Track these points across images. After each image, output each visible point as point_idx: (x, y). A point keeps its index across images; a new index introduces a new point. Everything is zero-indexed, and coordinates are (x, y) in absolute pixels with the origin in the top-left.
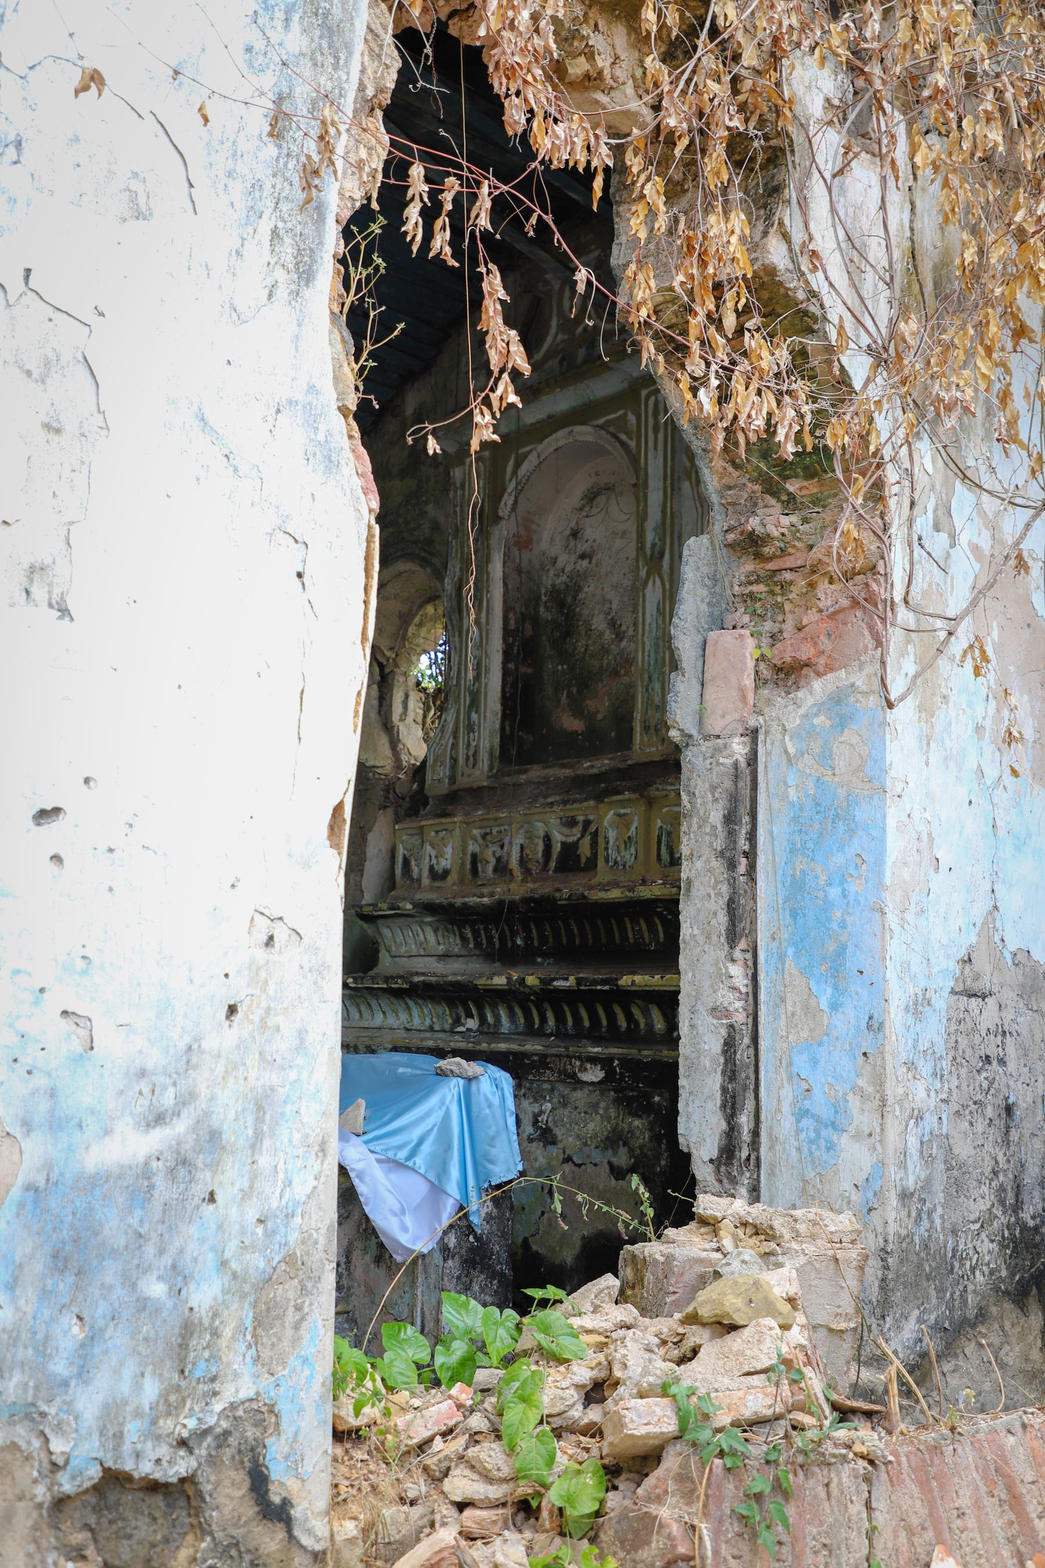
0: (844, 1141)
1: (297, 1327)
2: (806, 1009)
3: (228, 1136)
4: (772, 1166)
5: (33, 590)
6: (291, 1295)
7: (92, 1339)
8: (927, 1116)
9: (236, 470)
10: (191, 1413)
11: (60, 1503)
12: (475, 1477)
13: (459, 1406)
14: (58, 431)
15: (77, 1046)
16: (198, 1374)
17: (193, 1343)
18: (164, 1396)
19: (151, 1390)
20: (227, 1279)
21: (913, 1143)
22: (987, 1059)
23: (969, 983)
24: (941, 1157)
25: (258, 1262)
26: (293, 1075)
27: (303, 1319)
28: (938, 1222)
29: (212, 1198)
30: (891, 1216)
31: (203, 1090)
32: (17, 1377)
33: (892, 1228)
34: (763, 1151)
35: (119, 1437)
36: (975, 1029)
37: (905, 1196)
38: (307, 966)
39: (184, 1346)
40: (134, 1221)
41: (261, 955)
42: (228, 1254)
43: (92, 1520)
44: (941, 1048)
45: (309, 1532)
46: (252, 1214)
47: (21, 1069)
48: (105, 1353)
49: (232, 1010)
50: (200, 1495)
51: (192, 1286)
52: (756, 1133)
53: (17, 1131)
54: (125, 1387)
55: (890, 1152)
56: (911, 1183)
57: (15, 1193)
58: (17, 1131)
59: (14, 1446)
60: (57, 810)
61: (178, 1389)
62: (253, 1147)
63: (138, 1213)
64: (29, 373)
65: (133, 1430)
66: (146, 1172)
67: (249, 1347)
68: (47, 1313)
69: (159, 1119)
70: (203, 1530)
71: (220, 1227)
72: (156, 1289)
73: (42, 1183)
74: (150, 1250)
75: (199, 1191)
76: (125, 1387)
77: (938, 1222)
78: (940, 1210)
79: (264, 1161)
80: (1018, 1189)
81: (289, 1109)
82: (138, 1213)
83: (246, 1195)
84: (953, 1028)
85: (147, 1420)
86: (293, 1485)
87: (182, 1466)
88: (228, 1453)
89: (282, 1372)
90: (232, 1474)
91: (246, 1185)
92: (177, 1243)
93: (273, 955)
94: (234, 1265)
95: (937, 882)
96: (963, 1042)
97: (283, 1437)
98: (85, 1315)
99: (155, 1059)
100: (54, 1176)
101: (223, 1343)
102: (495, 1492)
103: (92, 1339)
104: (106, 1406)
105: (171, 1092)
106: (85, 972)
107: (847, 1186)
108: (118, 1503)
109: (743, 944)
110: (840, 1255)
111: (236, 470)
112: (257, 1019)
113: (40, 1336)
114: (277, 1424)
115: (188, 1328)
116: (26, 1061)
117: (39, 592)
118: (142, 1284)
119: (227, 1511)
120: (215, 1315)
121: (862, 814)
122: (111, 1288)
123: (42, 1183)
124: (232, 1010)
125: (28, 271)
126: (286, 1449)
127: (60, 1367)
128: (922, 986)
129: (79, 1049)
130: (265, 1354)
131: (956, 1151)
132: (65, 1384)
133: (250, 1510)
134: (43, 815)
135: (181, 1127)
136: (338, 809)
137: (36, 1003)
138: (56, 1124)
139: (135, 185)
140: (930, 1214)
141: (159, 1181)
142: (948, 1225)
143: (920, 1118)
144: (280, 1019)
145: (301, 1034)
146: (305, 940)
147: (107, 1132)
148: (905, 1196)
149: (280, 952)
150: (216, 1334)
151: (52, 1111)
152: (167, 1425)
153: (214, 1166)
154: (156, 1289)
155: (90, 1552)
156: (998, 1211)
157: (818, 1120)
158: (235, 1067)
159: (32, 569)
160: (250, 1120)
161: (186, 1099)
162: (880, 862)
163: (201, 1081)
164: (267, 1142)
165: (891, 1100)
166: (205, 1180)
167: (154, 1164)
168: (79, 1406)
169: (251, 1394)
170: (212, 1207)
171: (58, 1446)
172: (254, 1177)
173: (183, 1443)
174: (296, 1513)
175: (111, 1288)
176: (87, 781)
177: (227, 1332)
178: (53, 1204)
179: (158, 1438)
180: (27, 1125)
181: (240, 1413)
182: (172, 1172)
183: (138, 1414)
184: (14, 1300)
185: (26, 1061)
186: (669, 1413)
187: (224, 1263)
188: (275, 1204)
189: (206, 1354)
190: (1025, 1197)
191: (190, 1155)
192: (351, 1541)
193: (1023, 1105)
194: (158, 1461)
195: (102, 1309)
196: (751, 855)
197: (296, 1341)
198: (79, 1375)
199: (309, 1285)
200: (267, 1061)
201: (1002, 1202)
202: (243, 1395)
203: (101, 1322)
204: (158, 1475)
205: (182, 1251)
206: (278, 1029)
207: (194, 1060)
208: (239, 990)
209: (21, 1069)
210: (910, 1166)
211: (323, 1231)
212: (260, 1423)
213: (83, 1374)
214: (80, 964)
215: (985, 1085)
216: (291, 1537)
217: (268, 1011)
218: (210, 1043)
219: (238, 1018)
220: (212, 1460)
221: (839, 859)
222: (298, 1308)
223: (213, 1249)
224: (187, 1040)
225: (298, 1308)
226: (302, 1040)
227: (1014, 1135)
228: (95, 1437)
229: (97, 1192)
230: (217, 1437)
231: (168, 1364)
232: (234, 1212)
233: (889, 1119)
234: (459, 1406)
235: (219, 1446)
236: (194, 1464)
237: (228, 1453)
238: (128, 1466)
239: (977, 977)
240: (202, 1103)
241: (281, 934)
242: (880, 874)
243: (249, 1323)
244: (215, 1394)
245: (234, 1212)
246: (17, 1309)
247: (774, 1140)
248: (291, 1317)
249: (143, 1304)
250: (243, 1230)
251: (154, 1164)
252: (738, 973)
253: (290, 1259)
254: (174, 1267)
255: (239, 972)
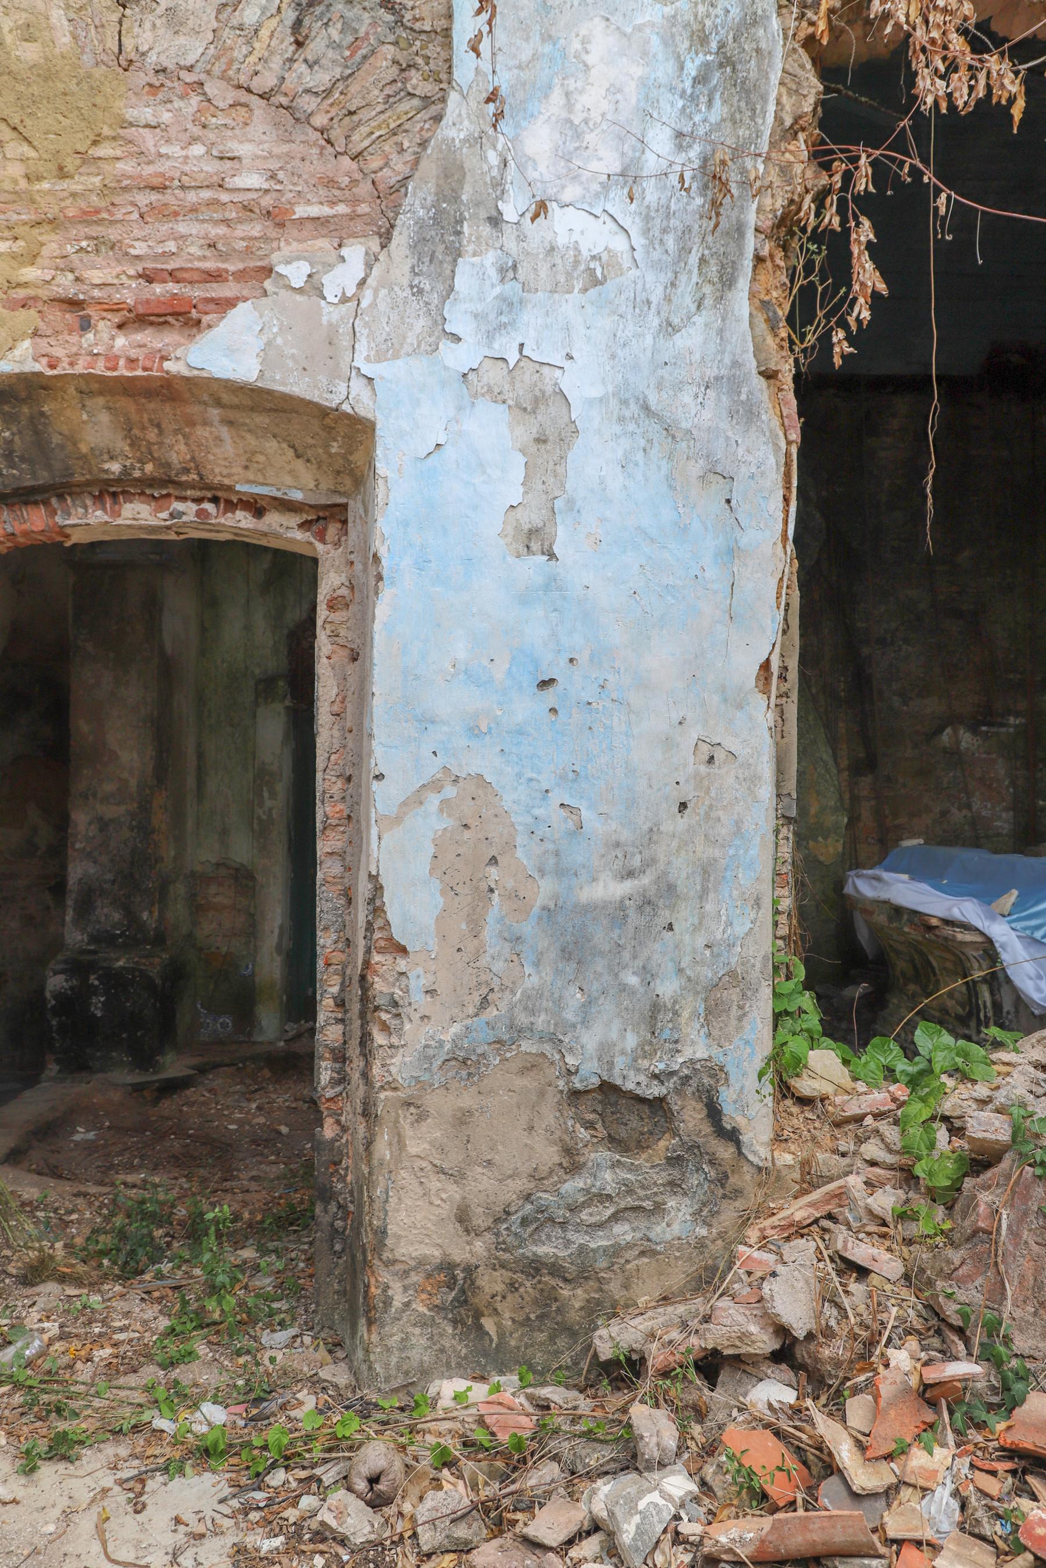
1: (740, 1019)
3: (681, 888)
5: (532, 544)
6: (734, 997)
7: (590, 1003)
9: (673, 437)
10: (661, 1059)
11: (575, 1094)
12: (882, 1146)
13: (894, 1100)
14: (545, 441)
15: (571, 825)
16: (665, 1036)
17: (660, 1017)
18: (641, 1045)
19: (631, 1041)
20: (683, 981)
25: (707, 974)
26: (731, 852)
27: (744, 1015)
29: (670, 927)
31: (662, 858)
32: (543, 1017)
35: (611, 1064)
38: (741, 776)
39: (653, 1017)
40: (615, 936)
41: (703, 769)
42: (683, 965)
43: (599, 1109)
45: (755, 1153)
46: (701, 941)
47: (536, 838)
48: (599, 1012)
49: (683, 806)
50: (670, 1110)
51: (658, 982)
53: (536, 875)
54: (614, 1035)
57: (536, 910)
58: (536, 875)
59: (543, 1055)
60: (552, 681)
61: (651, 1043)
62: (701, 898)
63: (617, 931)
64: (525, 409)
65: (620, 1062)
66: (621, 906)
67: (702, 1026)
68: (560, 983)
69: (630, 874)
70: (675, 1133)
71: (677, 947)
72: (633, 980)
73: (552, 906)
74: (626, 955)
75: (661, 921)
76: (614, 1035)
79: (709, 907)
81: (728, 874)
82: (617, 931)
83: (696, 929)
85: (630, 1058)
86: (741, 1121)
87: (655, 1090)
88: (689, 1090)
89: (728, 1046)
90: (694, 1103)
91: (696, 922)
92: (645, 953)
93: (714, 770)
94: (688, 972)
97: (731, 1089)
98: (584, 987)
99: (625, 835)
100: (560, 903)
101: (683, 1020)
102: (890, 1159)
103: (590, 1003)
104: (601, 1044)
105: (638, 857)
106: (575, 780)
108: (616, 1104)
111: (673, 437)
112: (702, 812)
113: (556, 995)
114: (727, 1080)
115: (656, 1008)
116: (539, 833)
117: (535, 546)
118: (622, 975)
119: (690, 1125)
120: (675, 1002)
122: (601, 974)
123: (552, 906)
124: (683, 806)
125: (522, 345)
126: (735, 1097)
127: (569, 1015)
129: (573, 828)
130: (715, 1033)
132: (574, 1026)
133: (707, 1129)
134: (546, 684)
135: (646, 880)
136: (766, 666)
137: (544, 799)
138: (560, 872)
139: (592, 266)
141: (632, 913)
144: (720, 813)
145: (738, 824)
146: (740, 759)
147: (594, 880)
149: (719, 768)
150: (676, 1013)
151: (557, 864)
152: (644, 1063)
153: (672, 908)
154: (633, 980)
155: (599, 1126)
158: (686, 844)
159: (530, 532)
160: (698, 880)
161: (649, 863)
163: (660, 852)
164: (711, 895)
166: (665, 916)
167: (627, 902)
168: (584, 1040)
169: (706, 1056)
170: (670, 933)
171: (570, 1060)
172: (702, 917)
173: (655, 1076)
174: (744, 1138)
175: (601, 974)
176: (571, 660)
177: (686, 1014)
178: (560, 919)
179: (638, 1070)
180: (542, 872)
181: (698, 1066)
182: (640, 908)
183: (623, 1053)
184: (539, 972)
185: (539, 833)
186: (1006, 1127)
187: (681, 971)
188: (719, 937)
189: (670, 1025)
191: (653, 899)
192: (789, 1167)
194: (638, 1083)
195: (596, 986)
197: (739, 1029)
198: (583, 1023)
199: (749, 993)
200: (711, 841)
202: (699, 1055)
203: (595, 994)
204: (638, 1092)
205: (649, 959)
206: (719, 820)
207: (655, 838)
208: (688, 792)
209: (536, 838)
211: (759, 959)
212: (713, 1076)
213: (585, 1022)
214: (571, 775)
216: (740, 1153)
217: (711, 807)
218: (667, 827)
219: (687, 812)
220: (678, 1091)
222: (741, 1007)
223: (672, 960)
224: (649, 825)
225: (741, 1007)
226: (739, 828)
228: (595, 1061)
229: (589, 915)
230: (681, 1078)
231: (643, 1027)
232: (687, 938)
234: (894, 1100)
235: (683, 1084)
236: (665, 1092)
237: (689, 1090)
238: (618, 1082)
240: (661, 866)
241: (720, 755)
243: (701, 1010)
244: (678, 1051)
245: (687, 938)
246: (541, 978)
248: (734, 1012)
249: (623, 988)
250: (694, 951)
251: (627, 902)
253: (732, 974)
254: (644, 967)
255: (687, 781)
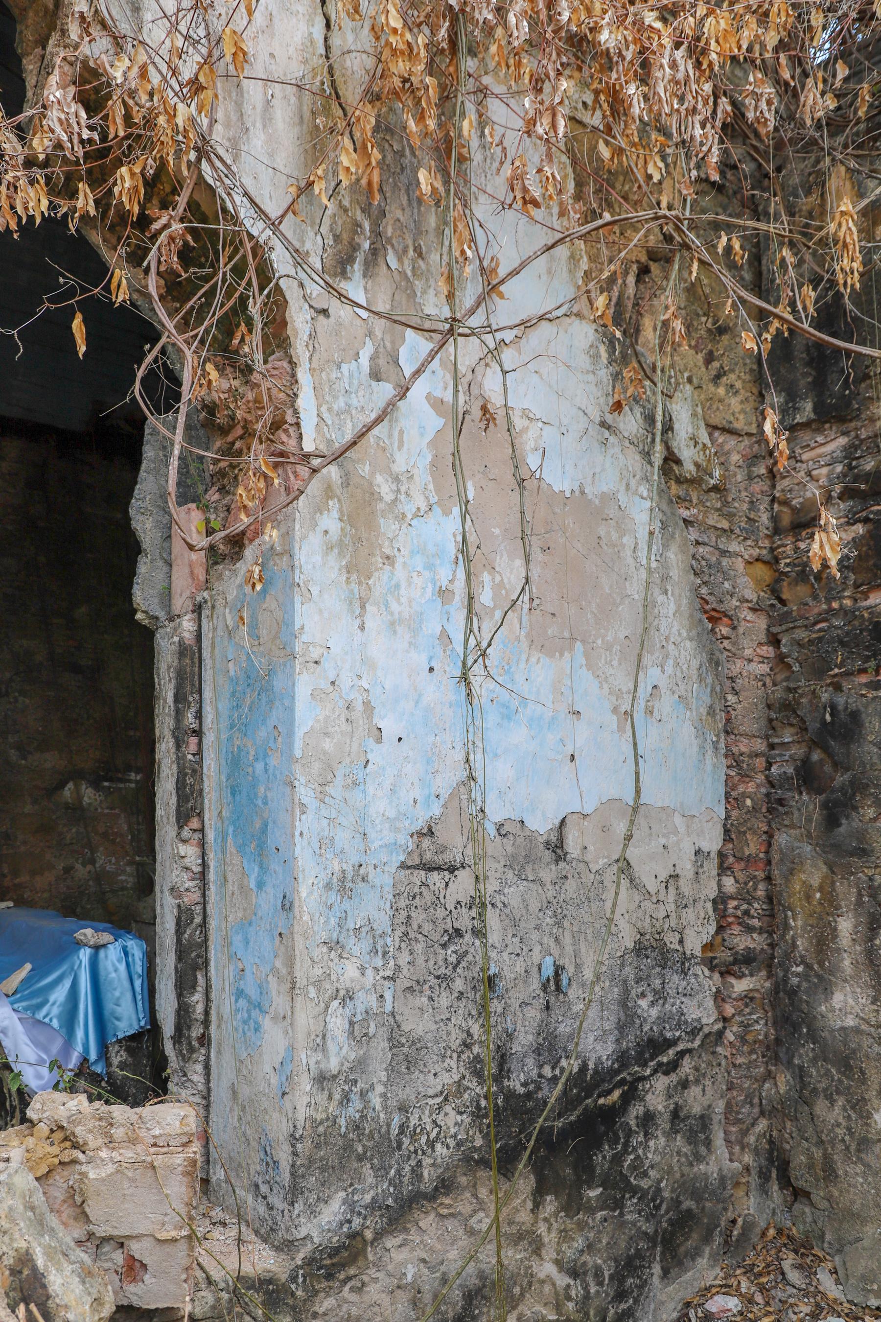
0: (266, 1023)
2: (241, 887)
4: (219, 1044)
8: (360, 996)
21: (337, 1023)
22: (458, 933)
23: (428, 856)
24: (383, 1033)
28: (376, 1101)
30: (302, 1101)
33: (301, 1114)
34: (213, 1028)
36: (437, 901)
37: (322, 1079)
44: (382, 922)
52: (207, 1013)
55: (301, 1036)
56: (333, 1065)
77: (376, 1101)
78: (379, 1089)
80: (503, 1058)
84: (403, 903)
95: (377, 755)
96: (418, 917)
107: (268, 1068)
109: (195, 823)
110: (159, 1161)
121: (278, 683)
128: (355, 860)
131: (406, 1027)
140: (363, 1094)
142: (393, 1103)
143: (349, 996)
148: (322, 1079)
156: (472, 1083)
157: (249, 1001)
162: (291, 734)
165: (301, 982)
190: (514, 1065)
193: (508, 974)
196: (198, 733)
201: (478, 1074)
210: (332, 1047)
215: (453, 959)
221: (262, 733)
227: (496, 1006)
233: (299, 1000)
239: (443, 849)
242: (290, 745)
247: (220, 1018)
252: (190, 852)
